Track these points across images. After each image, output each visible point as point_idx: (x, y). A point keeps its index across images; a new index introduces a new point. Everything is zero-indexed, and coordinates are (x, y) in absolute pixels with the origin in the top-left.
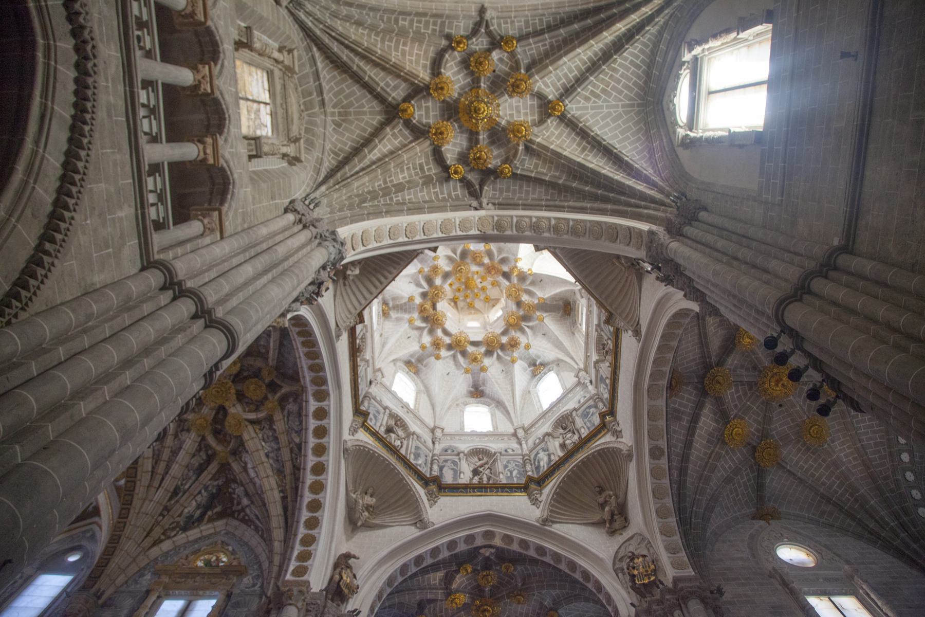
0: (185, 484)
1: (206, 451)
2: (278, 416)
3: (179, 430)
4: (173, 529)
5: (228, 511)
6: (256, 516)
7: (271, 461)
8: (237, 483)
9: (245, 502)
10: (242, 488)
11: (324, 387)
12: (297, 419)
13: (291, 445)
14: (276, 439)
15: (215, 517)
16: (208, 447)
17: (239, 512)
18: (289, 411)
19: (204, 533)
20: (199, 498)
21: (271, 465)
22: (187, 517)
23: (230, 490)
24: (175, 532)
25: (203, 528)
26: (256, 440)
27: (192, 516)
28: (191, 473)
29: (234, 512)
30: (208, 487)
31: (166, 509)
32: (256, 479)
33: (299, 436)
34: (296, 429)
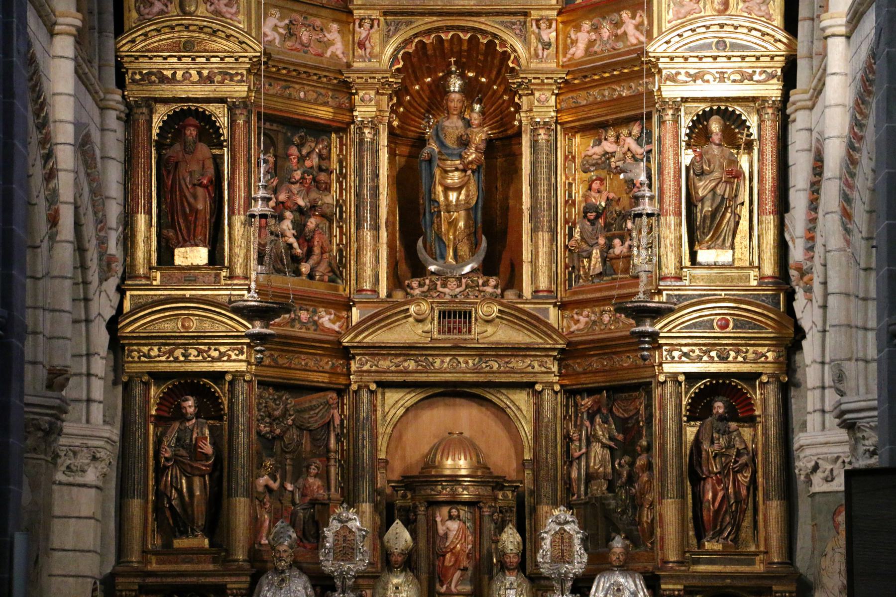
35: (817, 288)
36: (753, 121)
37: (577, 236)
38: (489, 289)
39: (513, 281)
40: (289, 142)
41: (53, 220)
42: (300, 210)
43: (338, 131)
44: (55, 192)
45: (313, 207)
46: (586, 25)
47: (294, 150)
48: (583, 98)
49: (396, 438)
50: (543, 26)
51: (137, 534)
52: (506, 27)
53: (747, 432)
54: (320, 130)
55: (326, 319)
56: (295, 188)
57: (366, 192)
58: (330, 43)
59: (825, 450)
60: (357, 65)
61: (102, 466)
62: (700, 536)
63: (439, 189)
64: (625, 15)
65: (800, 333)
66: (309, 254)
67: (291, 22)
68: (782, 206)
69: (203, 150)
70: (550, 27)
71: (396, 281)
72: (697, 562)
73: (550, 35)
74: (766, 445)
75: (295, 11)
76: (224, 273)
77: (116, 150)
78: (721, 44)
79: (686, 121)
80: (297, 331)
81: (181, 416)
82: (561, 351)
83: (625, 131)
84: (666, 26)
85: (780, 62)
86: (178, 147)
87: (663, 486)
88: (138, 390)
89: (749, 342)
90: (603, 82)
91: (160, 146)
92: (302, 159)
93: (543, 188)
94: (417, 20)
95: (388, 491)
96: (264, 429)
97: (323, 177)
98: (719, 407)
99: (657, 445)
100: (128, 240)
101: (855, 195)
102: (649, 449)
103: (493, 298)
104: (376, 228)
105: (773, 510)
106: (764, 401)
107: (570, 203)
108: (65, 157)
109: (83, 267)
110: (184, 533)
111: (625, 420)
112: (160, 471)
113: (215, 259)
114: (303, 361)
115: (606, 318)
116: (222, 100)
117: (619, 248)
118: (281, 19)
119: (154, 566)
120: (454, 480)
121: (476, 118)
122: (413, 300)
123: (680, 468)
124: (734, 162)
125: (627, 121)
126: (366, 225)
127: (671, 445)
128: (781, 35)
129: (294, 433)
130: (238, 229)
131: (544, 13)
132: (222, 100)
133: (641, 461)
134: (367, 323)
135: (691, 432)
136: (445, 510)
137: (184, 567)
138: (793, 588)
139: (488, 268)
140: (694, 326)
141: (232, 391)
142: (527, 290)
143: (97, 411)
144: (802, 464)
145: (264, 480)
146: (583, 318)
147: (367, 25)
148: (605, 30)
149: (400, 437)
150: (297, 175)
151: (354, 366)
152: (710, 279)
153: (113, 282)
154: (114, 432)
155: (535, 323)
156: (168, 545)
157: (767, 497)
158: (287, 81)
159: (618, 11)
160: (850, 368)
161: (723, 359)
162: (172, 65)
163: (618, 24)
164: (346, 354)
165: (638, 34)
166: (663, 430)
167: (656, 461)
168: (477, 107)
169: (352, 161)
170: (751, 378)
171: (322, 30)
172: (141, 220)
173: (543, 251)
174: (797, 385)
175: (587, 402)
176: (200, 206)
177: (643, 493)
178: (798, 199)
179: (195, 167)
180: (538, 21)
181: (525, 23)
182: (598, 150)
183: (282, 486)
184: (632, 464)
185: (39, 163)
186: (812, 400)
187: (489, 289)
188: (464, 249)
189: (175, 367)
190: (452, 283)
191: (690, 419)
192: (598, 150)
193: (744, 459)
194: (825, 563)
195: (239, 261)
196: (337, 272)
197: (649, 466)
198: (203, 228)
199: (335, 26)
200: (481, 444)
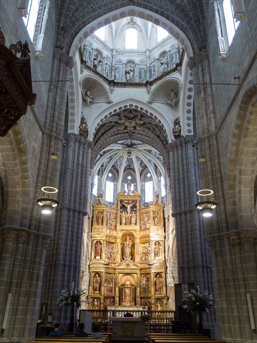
35: (169, 262)
36: (161, 243)
37: (142, 255)
38: (132, 262)
39: (134, 261)
40: (109, 244)
41: (84, 254)
42: (110, 252)
43: (115, 243)
44: (84, 250)
45: (112, 252)
46: (143, 232)
47: (110, 245)
48: (142, 240)
49: (121, 279)
51: (91, 291)
53: (161, 279)
54: (113, 243)
55: (113, 265)
56: (110, 250)
57: (118, 250)
58: (114, 233)
59: (171, 281)
60: (117, 236)
61: (87, 283)
62: (156, 291)
63: (126, 250)
64: (147, 231)
65: (167, 267)
66: (111, 257)
68: (165, 252)
69: (100, 245)
71: (121, 261)
72: (156, 295)
73: (138, 233)
74: (164, 280)
76: (102, 260)
77: (90, 245)
78: (157, 234)
79: (154, 243)
80: (110, 266)
81: (96, 277)
82: (140, 269)
83: (147, 244)
84: (151, 232)
85: (164, 236)
86: (97, 245)
87: (152, 286)
88: (91, 273)
89: (161, 268)
90: (145, 238)
91: (95, 245)
92: (111, 246)
93: (138, 250)
95: (120, 286)
96: (106, 278)
97: (113, 248)
98: (158, 276)
99: (151, 281)
100: (91, 256)
101: (173, 251)
102: (150, 281)
103: (132, 263)
104: (119, 254)
105: (164, 288)
106: (163, 275)
107: (141, 252)
108: (85, 246)
109: (86, 259)
110: (96, 291)
111: (147, 278)
112: (93, 283)
113: (101, 258)
114: (110, 270)
115: (145, 265)
116: (102, 240)
117: (146, 257)
119: (92, 295)
120: (128, 285)
121: (130, 242)
122: (123, 263)
123: (154, 283)
124: (159, 247)
125: (148, 242)
126: (118, 254)
127: (153, 281)
128: (164, 233)
129: (109, 279)
130: (104, 255)
132: (102, 240)
133: (149, 282)
134: (118, 266)
135: (155, 279)
136: (126, 288)
137: (96, 295)
138: (167, 298)
139: (132, 259)
140: (155, 266)
141: (102, 274)
142: (136, 262)
143: (87, 276)
144: (168, 283)
145: (105, 285)
146: (143, 265)
149: (121, 280)
150: (110, 248)
151: (116, 271)
152: (157, 261)
153: (89, 260)
154: (89, 279)
155: (137, 266)
156: (94, 292)
157: (164, 287)
158: (110, 238)
160: (173, 271)
161: (159, 270)
162: (97, 236)
163: (146, 232)
164: (115, 269)
166: (152, 279)
167: (151, 283)
168: (130, 241)
169: (116, 246)
170: (162, 272)
172: (93, 253)
173: (138, 257)
174: (167, 273)
175: (143, 275)
176: (99, 252)
177: (150, 286)
178: (166, 252)
179: (99, 247)
182: (144, 246)
183: (107, 285)
184: (148, 283)
185: (83, 247)
186: (169, 275)
187: (132, 262)
188: (129, 257)
189: (96, 271)
190: (127, 261)
191: (155, 277)
192: (144, 246)
193: (161, 282)
194: (171, 295)
195: (103, 258)
196: (114, 260)
197: (150, 283)
198: (99, 255)
199: (115, 232)
200: (130, 280)
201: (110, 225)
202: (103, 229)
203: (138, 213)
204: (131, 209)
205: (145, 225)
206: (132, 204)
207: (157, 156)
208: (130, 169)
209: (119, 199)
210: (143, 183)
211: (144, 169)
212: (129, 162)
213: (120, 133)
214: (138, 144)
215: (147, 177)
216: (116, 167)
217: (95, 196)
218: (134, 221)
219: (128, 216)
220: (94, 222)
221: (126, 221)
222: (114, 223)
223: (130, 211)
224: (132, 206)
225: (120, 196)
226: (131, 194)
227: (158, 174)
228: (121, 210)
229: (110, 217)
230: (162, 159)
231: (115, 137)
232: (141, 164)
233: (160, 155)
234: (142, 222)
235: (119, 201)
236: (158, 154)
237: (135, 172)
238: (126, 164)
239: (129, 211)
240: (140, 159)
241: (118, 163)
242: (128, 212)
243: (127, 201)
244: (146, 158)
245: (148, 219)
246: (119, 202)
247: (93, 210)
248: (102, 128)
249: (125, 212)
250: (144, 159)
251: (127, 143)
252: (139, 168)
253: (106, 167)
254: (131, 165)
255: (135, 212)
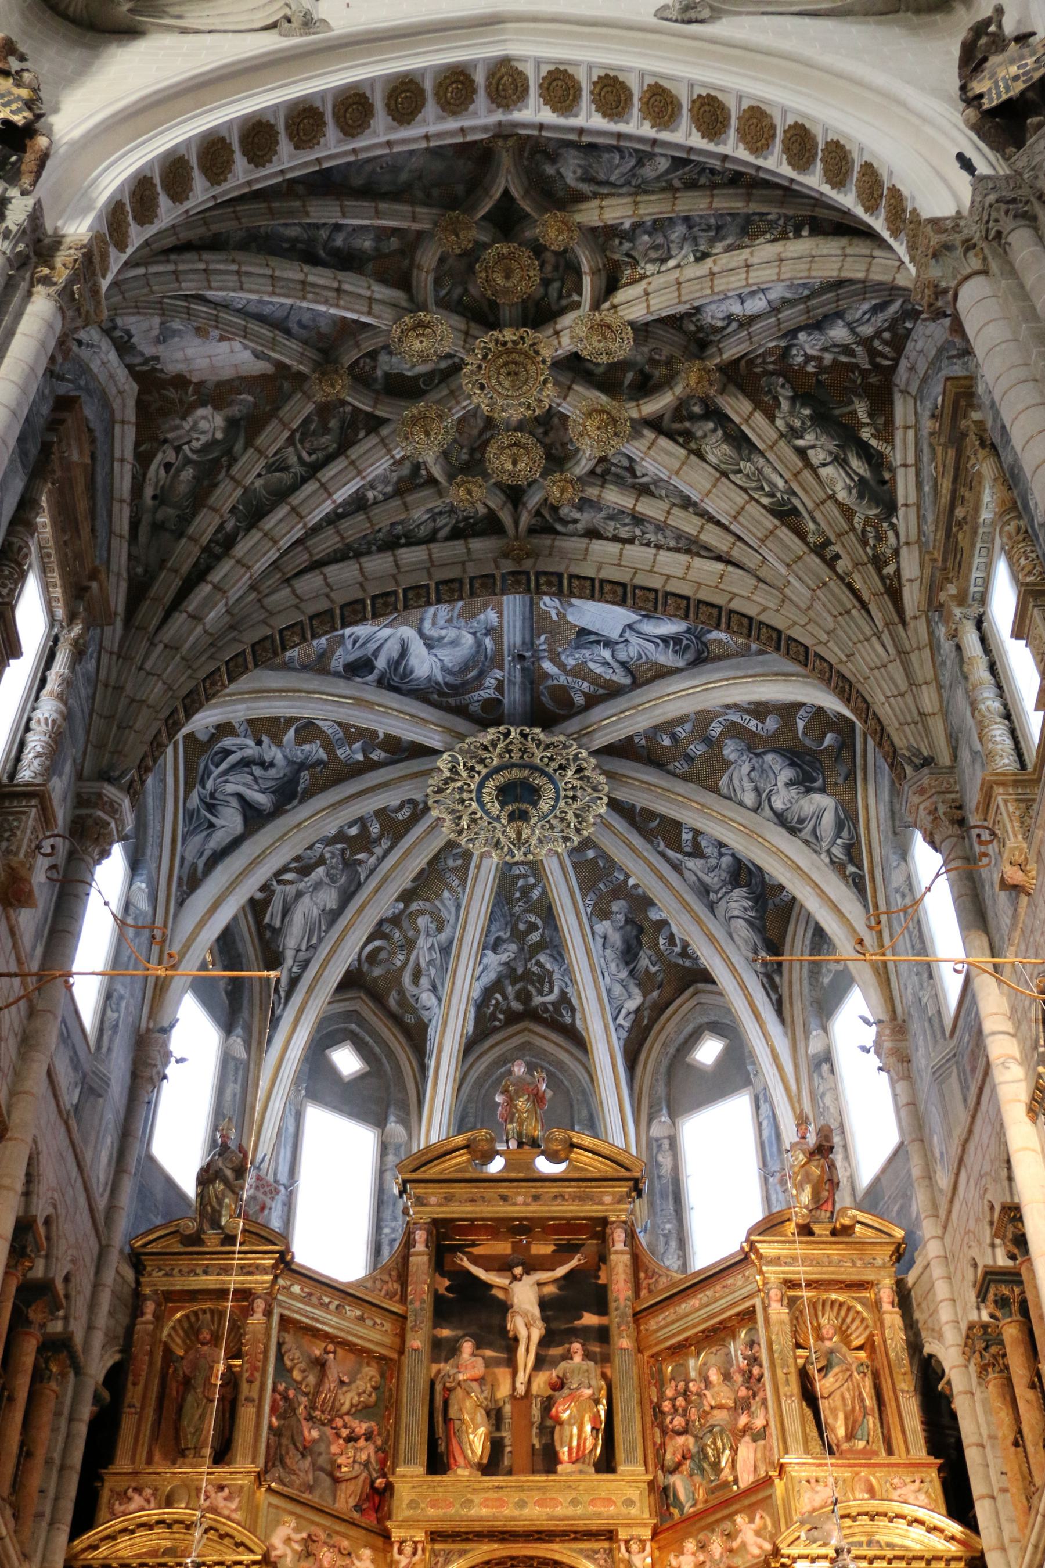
0: (772, 484)
1: (693, 418)
2: (590, 215)
3: (630, 480)
4: (880, 538)
5: (873, 380)
6: (876, 309)
7: (719, 247)
8: (788, 348)
9: (839, 333)
10: (802, 336)
11: (480, 78)
12: (606, 156)
13: (677, 183)
14: (660, 226)
15: (881, 421)
16: (680, 410)
17: (873, 353)
18: (582, 180)
19: (911, 460)
20: (817, 457)
21: (729, 249)
22: (861, 496)
23: (810, 369)
24: (891, 534)
25: (898, 461)
26: (658, 281)
27: (862, 479)
28: (747, 467)
29: (876, 367)
30: (791, 428)
31: (820, 550)
32: (773, 295)
33: (651, 156)
34: (633, 162)
46: (690, 1545)
50: (634, 1547)
52: (587, 1557)
67: (309, 1536)
70: (643, 1550)
75: (317, 1524)
94: (473, 1549)
118: (297, 1530)
131: (637, 1531)
147: (408, 1549)
148: (716, 1545)
159: (730, 1517)
165: (760, 1541)
171: (349, 1554)
180: (627, 1542)
181: (611, 1550)
199: (367, 1553)
201: (316, 1467)
202: (219, 1499)
203: (625, 1343)
204: (545, 1319)
205: (716, 1466)
206: (561, 1271)
207: (778, 804)
208: (532, 1015)
209: (423, 1215)
210: (658, 1130)
211: (659, 1009)
212: (518, 937)
213: (423, 532)
214: (592, 701)
215: (695, 1070)
216: (401, 992)
217: (170, 1184)
218: (588, 1428)
219: (521, 1389)
220: (128, 1425)
221: (496, 1446)
222: (367, 1451)
223: (536, 1334)
224: (550, 1290)
225: (431, 1188)
226: (544, 1166)
227: (798, 1009)
228: (445, 1333)
229: (320, 1383)
230: (828, 820)
231: (378, 564)
232: (629, 955)
233: (809, 791)
234: (681, 1440)
235: (420, 1236)
236: (790, 784)
237: (578, 1041)
238: (493, 960)
239: (523, 1333)
240: (620, 891)
241: (424, 952)
242: (510, 1344)
243: (503, 1248)
244: (677, 868)
245: (743, 1392)
246: (420, 1247)
247: (137, 1300)
248: (249, 444)
249: (489, 1353)
250: (661, 877)
251: (487, 692)
252: (617, 989)
253: (305, 964)
254: (543, 979)
255: (596, 1349)
